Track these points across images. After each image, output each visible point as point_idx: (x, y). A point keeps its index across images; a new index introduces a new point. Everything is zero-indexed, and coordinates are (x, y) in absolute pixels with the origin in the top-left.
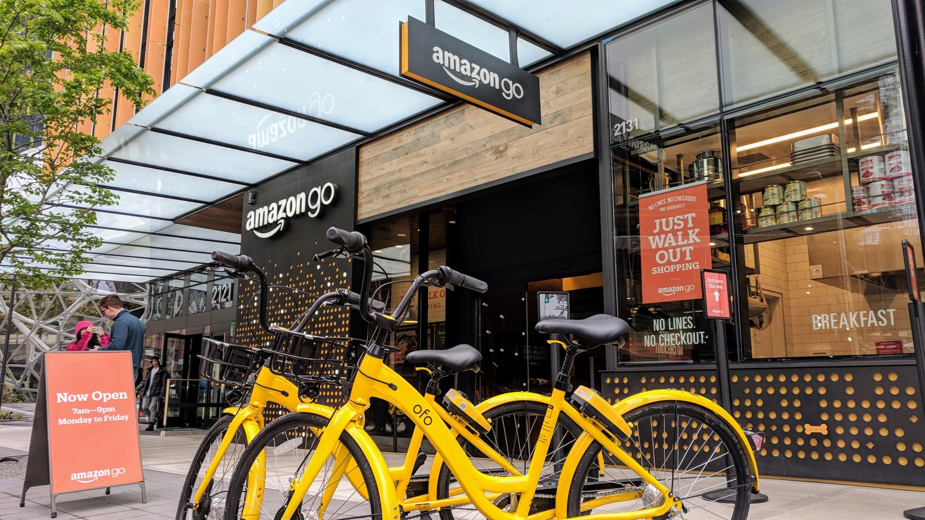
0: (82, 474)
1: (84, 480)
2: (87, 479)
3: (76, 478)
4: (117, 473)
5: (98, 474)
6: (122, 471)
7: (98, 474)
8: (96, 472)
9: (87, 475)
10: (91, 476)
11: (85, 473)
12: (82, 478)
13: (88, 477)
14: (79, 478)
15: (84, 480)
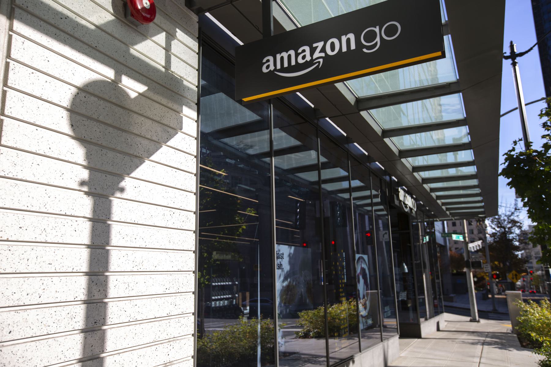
0: (285, 55)
1: (291, 69)
2: (299, 67)
3: (272, 68)
4: (378, 39)
5: (323, 50)
6: (391, 31)
7: (323, 50)
8: (320, 45)
9: (297, 55)
10: (308, 58)
11: (292, 53)
12: (286, 65)
13: (300, 61)
14: (279, 67)
15: (291, 69)
